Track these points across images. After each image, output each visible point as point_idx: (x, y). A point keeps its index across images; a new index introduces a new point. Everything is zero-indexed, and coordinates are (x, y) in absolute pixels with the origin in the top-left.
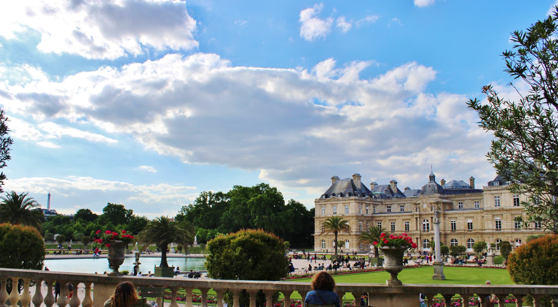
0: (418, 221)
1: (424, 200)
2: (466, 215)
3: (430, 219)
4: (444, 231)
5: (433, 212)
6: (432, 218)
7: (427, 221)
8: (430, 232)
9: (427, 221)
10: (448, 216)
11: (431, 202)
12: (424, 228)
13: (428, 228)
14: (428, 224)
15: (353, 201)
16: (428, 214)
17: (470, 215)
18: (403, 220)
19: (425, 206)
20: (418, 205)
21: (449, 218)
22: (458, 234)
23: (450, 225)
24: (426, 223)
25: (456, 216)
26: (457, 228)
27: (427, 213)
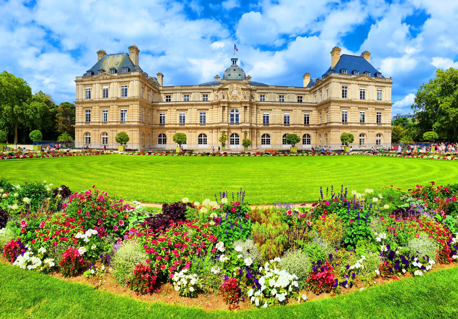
0: (226, 110)
1: (235, 85)
2: (283, 108)
3: (241, 110)
4: (257, 124)
5: (245, 100)
6: (246, 107)
7: (237, 111)
8: (240, 125)
9: (237, 111)
10: (260, 108)
11: (244, 87)
12: (232, 120)
13: (237, 120)
14: (237, 116)
15: (136, 78)
16: (241, 103)
17: (289, 108)
18: (198, 110)
19: (235, 93)
20: (226, 91)
21: (261, 110)
22: (273, 129)
23: (262, 118)
24: (235, 113)
25: (271, 107)
26: (270, 122)
27: (238, 101)
